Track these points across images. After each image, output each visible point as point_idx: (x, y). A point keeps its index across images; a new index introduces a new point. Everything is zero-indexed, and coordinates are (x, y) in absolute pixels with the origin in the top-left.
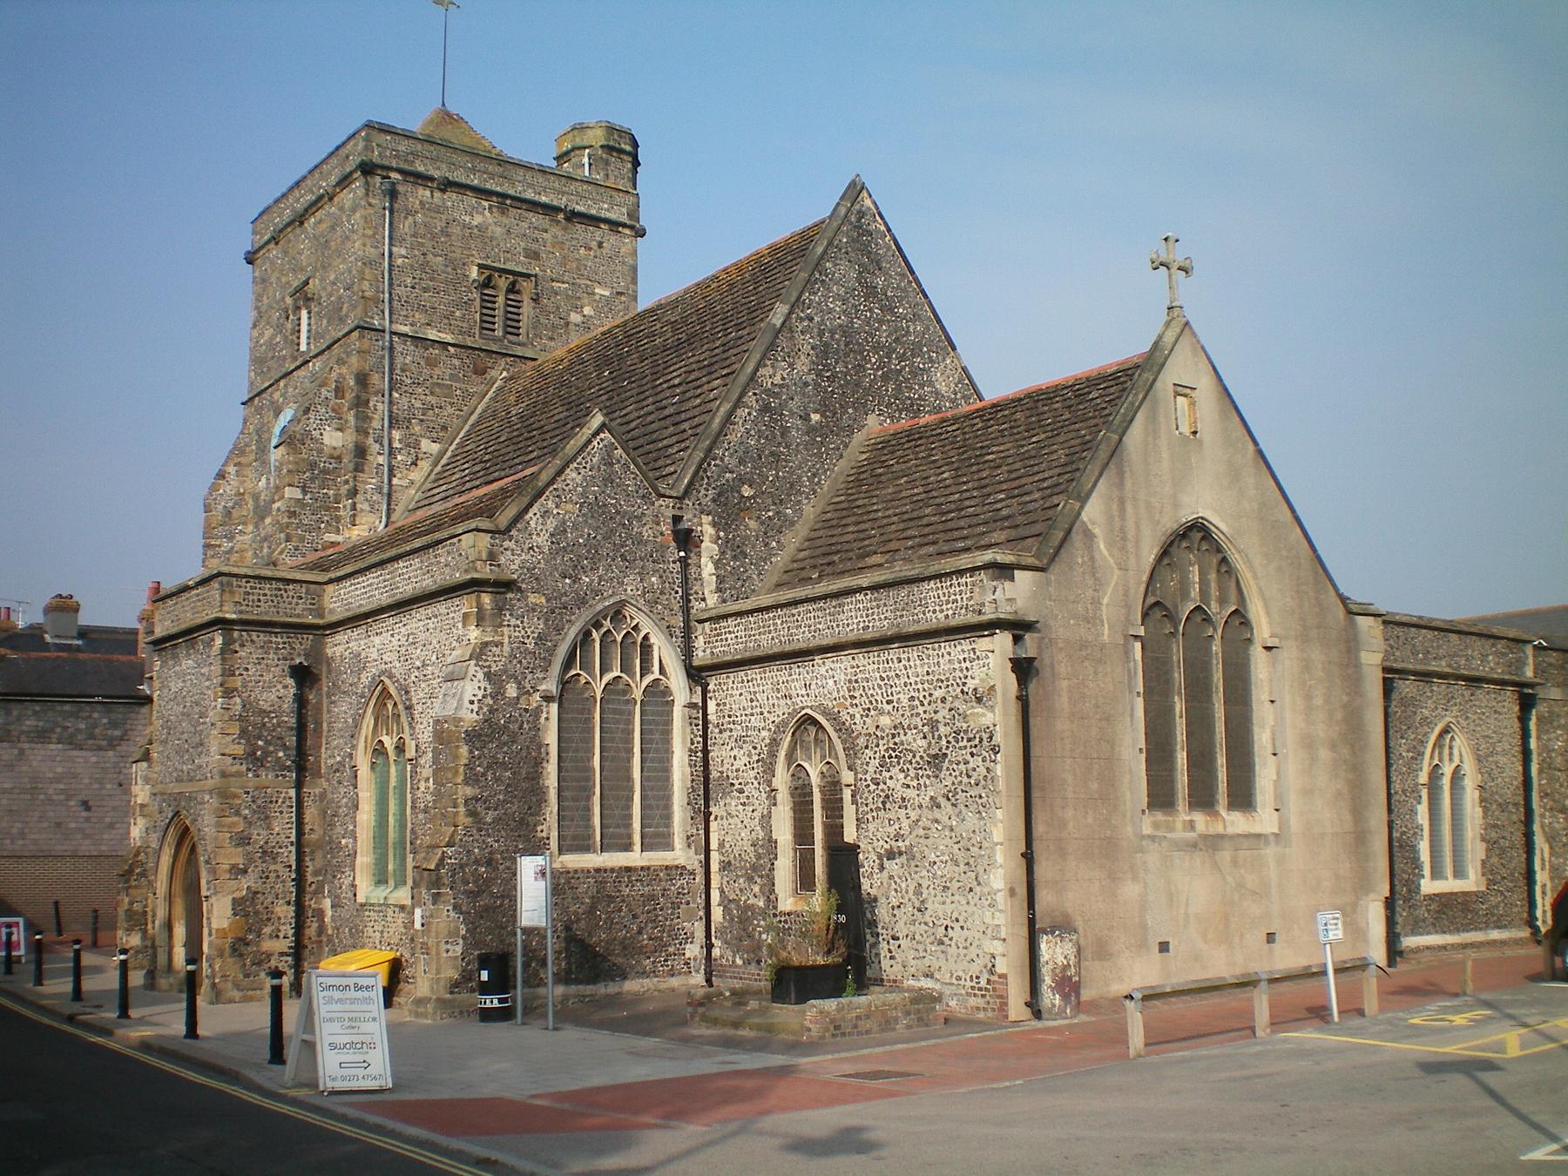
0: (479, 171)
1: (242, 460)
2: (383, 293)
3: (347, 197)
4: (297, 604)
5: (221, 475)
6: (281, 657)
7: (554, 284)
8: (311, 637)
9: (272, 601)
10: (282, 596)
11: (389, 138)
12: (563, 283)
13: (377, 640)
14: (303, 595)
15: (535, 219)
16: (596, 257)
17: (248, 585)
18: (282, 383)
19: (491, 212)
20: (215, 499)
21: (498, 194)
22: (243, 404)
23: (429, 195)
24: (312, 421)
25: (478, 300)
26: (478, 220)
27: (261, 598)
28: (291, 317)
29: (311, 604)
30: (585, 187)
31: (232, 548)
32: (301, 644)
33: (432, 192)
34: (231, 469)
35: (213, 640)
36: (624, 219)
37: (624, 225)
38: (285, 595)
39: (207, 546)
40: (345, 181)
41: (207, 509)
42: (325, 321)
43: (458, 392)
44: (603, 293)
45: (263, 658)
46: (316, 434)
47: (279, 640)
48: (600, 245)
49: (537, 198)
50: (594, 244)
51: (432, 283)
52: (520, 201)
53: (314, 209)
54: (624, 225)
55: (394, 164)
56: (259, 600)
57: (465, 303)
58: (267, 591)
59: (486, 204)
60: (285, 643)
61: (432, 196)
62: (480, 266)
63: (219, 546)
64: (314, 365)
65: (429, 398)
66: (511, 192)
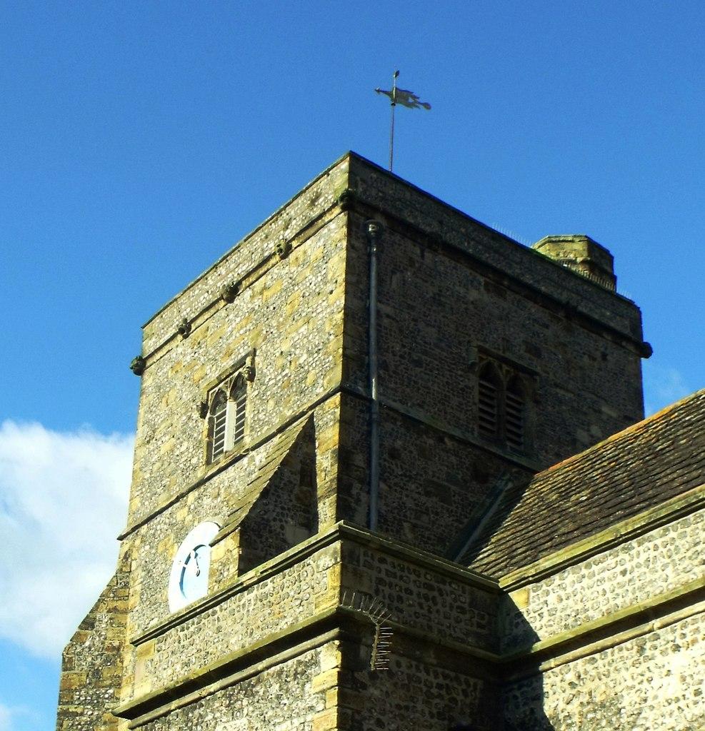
0: (473, 239)
1: (120, 605)
2: (368, 354)
3: (311, 248)
4: (458, 621)
5: (88, 623)
6: (435, 711)
7: (558, 390)
8: (480, 683)
9: (421, 605)
10: (434, 598)
11: (374, 176)
12: (567, 391)
13: (677, 662)
14: (466, 606)
15: (534, 309)
16: (600, 369)
17: (383, 567)
18: (192, 497)
19: (488, 290)
20: (79, 654)
21: (495, 270)
22: (121, 538)
23: (419, 252)
24: (271, 507)
25: (477, 389)
26: (473, 295)
27: (403, 595)
28: (208, 415)
29: (479, 626)
30: (586, 287)
31: (98, 717)
32: (465, 693)
33: (422, 251)
34: (103, 616)
35: (315, 662)
36: (627, 332)
37: (628, 339)
38: (439, 599)
39: (63, 715)
40: (311, 227)
41: (67, 664)
42: (271, 403)
43: (457, 497)
44: (609, 412)
45: (407, 708)
46: (276, 526)
47: (431, 678)
48: (604, 356)
49: (536, 285)
50: (598, 355)
51: (423, 357)
52: (517, 284)
53: (251, 279)
54: (628, 339)
55: (381, 205)
56: (400, 599)
57: (461, 389)
58: (412, 586)
59: (482, 280)
60: (440, 686)
61: (423, 256)
62: (482, 350)
63: (82, 714)
64: (253, 459)
65: (424, 499)
66: (509, 272)
